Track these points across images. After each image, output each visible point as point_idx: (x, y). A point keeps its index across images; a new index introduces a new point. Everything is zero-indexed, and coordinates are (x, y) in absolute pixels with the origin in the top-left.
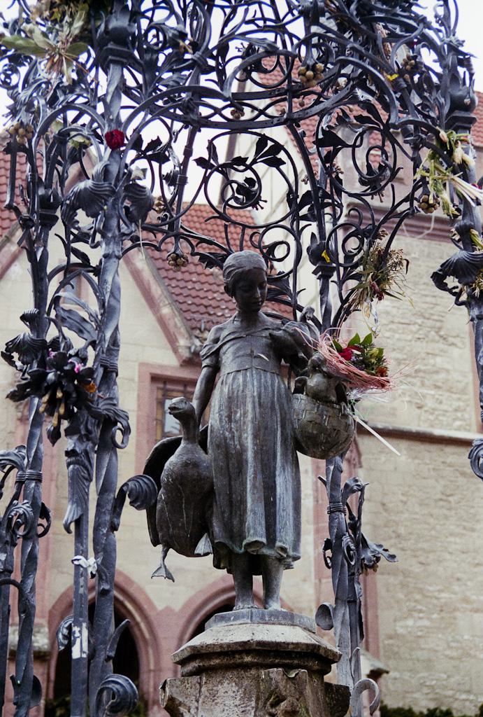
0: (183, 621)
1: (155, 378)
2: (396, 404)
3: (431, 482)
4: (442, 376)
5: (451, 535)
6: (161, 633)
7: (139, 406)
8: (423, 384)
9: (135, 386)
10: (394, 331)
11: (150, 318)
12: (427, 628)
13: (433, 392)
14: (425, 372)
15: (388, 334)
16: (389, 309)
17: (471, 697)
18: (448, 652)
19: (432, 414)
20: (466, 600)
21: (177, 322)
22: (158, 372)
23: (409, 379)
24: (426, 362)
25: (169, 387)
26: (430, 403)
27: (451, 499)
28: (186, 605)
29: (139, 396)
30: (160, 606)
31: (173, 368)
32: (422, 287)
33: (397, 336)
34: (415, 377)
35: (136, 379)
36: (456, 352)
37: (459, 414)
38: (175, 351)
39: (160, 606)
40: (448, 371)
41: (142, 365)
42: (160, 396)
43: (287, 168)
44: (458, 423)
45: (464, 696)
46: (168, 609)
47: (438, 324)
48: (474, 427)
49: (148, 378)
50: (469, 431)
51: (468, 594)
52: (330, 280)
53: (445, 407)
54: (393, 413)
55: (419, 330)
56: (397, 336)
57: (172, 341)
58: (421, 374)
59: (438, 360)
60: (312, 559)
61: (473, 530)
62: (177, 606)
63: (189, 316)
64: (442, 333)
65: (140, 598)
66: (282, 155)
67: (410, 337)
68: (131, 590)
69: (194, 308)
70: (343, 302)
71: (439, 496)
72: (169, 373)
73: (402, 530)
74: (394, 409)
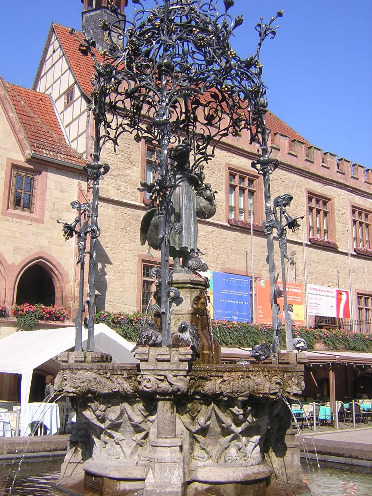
2: (109, 187)
3: (120, 221)
4: (128, 178)
5: (126, 243)
7: (6, 177)
8: (121, 180)
10: (112, 157)
11: (13, 139)
12: (113, 279)
13: (124, 184)
14: (122, 175)
15: (108, 158)
16: (110, 147)
17: (127, 307)
18: (120, 289)
19: (123, 193)
20: (129, 269)
23: (115, 178)
24: (122, 171)
26: (123, 188)
27: (127, 228)
28: (20, 263)
29: (6, 172)
31: (22, 162)
32: (124, 140)
33: (112, 159)
34: (117, 177)
35: (5, 165)
36: (135, 168)
37: (134, 194)
38: (23, 155)
40: (131, 176)
41: (8, 159)
43: (178, 110)
44: (133, 198)
45: (124, 306)
46: (13, 264)
47: (129, 156)
48: (139, 200)
50: (137, 202)
51: (130, 267)
52: (190, 153)
53: (128, 191)
54: (108, 191)
55: (121, 158)
56: (112, 159)
57: (23, 150)
58: (120, 176)
59: (128, 171)
60: (74, 248)
61: (134, 242)
62: (17, 264)
64: (130, 160)
66: (177, 105)
67: (117, 160)
70: (196, 162)
71: (122, 227)
73: (107, 239)
74: (108, 189)
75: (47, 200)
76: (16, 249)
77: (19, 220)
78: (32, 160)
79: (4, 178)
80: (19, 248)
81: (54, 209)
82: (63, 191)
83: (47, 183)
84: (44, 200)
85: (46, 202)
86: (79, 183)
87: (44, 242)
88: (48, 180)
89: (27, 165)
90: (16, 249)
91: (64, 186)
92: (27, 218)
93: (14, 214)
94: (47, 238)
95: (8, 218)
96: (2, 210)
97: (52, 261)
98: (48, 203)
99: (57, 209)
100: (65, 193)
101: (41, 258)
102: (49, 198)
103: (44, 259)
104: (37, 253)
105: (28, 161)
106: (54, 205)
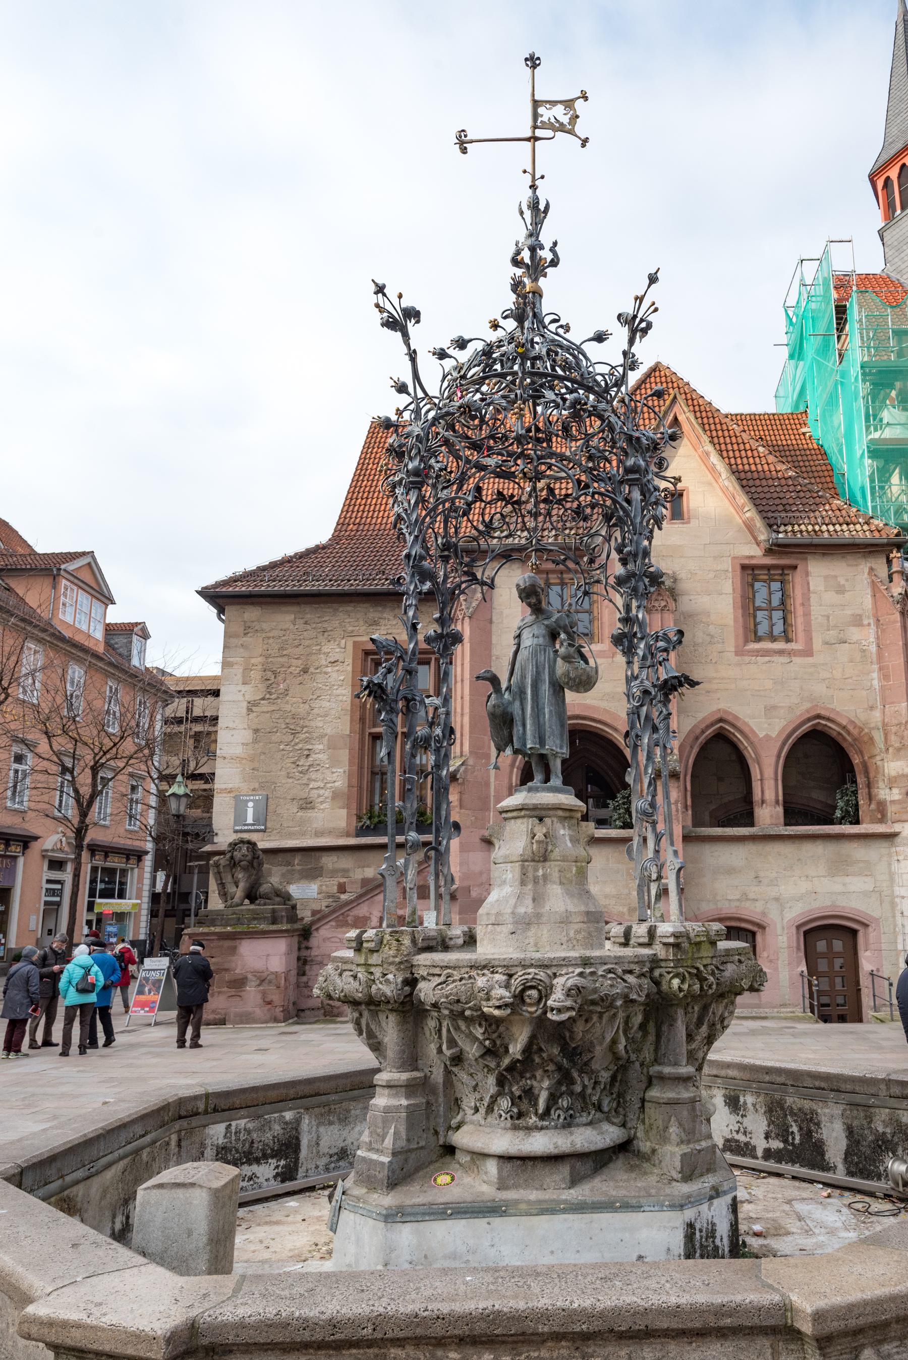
0: (778, 744)
1: (744, 567)
6: (763, 754)
7: (734, 589)
9: (730, 575)
21: (759, 523)
22: (747, 562)
25: (756, 572)
28: (780, 733)
30: (761, 735)
35: (730, 570)
38: (758, 544)
39: (761, 735)
41: (734, 558)
42: (750, 580)
46: (767, 736)
49: (738, 568)
63: (770, 515)
65: (746, 730)
68: (739, 724)
69: (773, 508)
72: (754, 562)
75: (812, 613)
76: (770, 709)
77: (767, 659)
78: (775, 549)
79: (731, 591)
80: (774, 707)
81: (828, 626)
82: (841, 590)
83: (808, 583)
84: (807, 614)
85: (813, 618)
86: (871, 569)
87: (820, 689)
88: (810, 578)
89: (768, 561)
90: (770, 709)
91: (842, 582)
92: (781, 652)
93: (758, 651)
94: (824, 680)
95: (747, 659)
96: (736, 647)
97: (839, 720)
98: (816, 618)
99: (836, 626)
100: (847, 595)
101: (818, 716)
102: (816, 611)
103: (823, 718)
104: (808, 711)
105: (769, 552)
106: (828, 620)
